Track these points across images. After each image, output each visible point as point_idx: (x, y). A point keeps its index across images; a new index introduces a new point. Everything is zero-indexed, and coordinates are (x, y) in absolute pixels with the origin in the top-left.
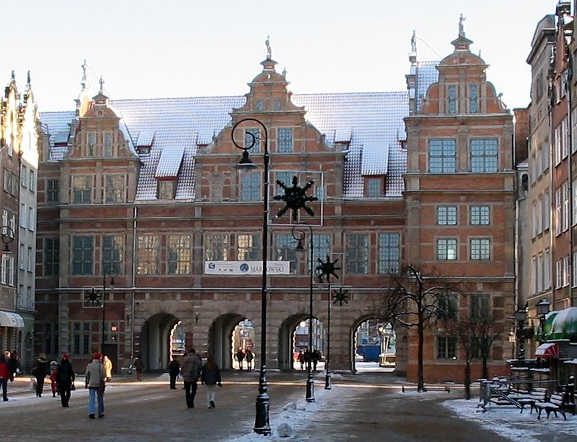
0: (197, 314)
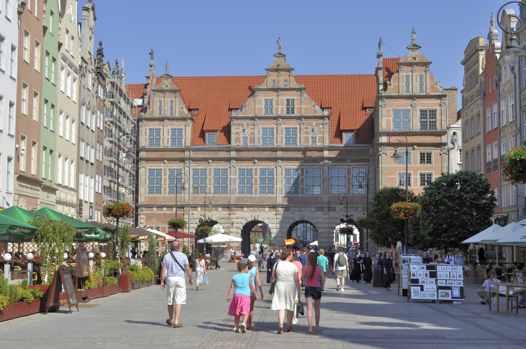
0: (232, 220)
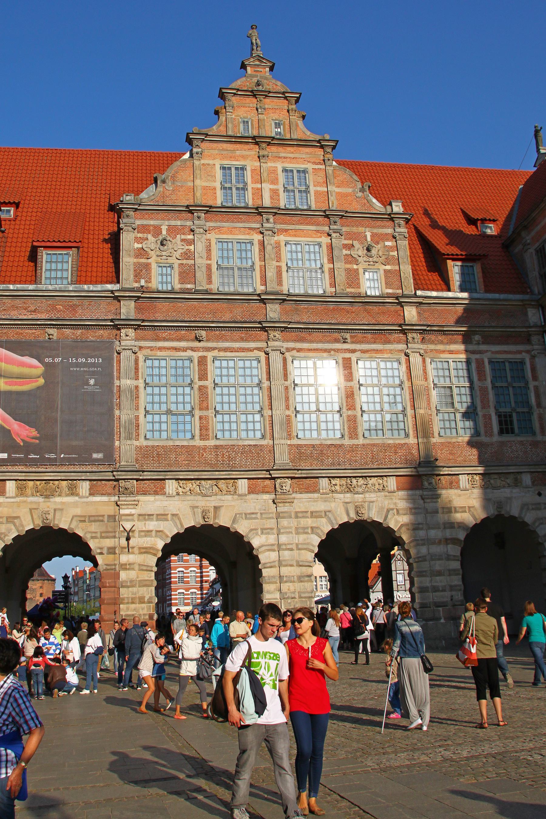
0: (128, 526)
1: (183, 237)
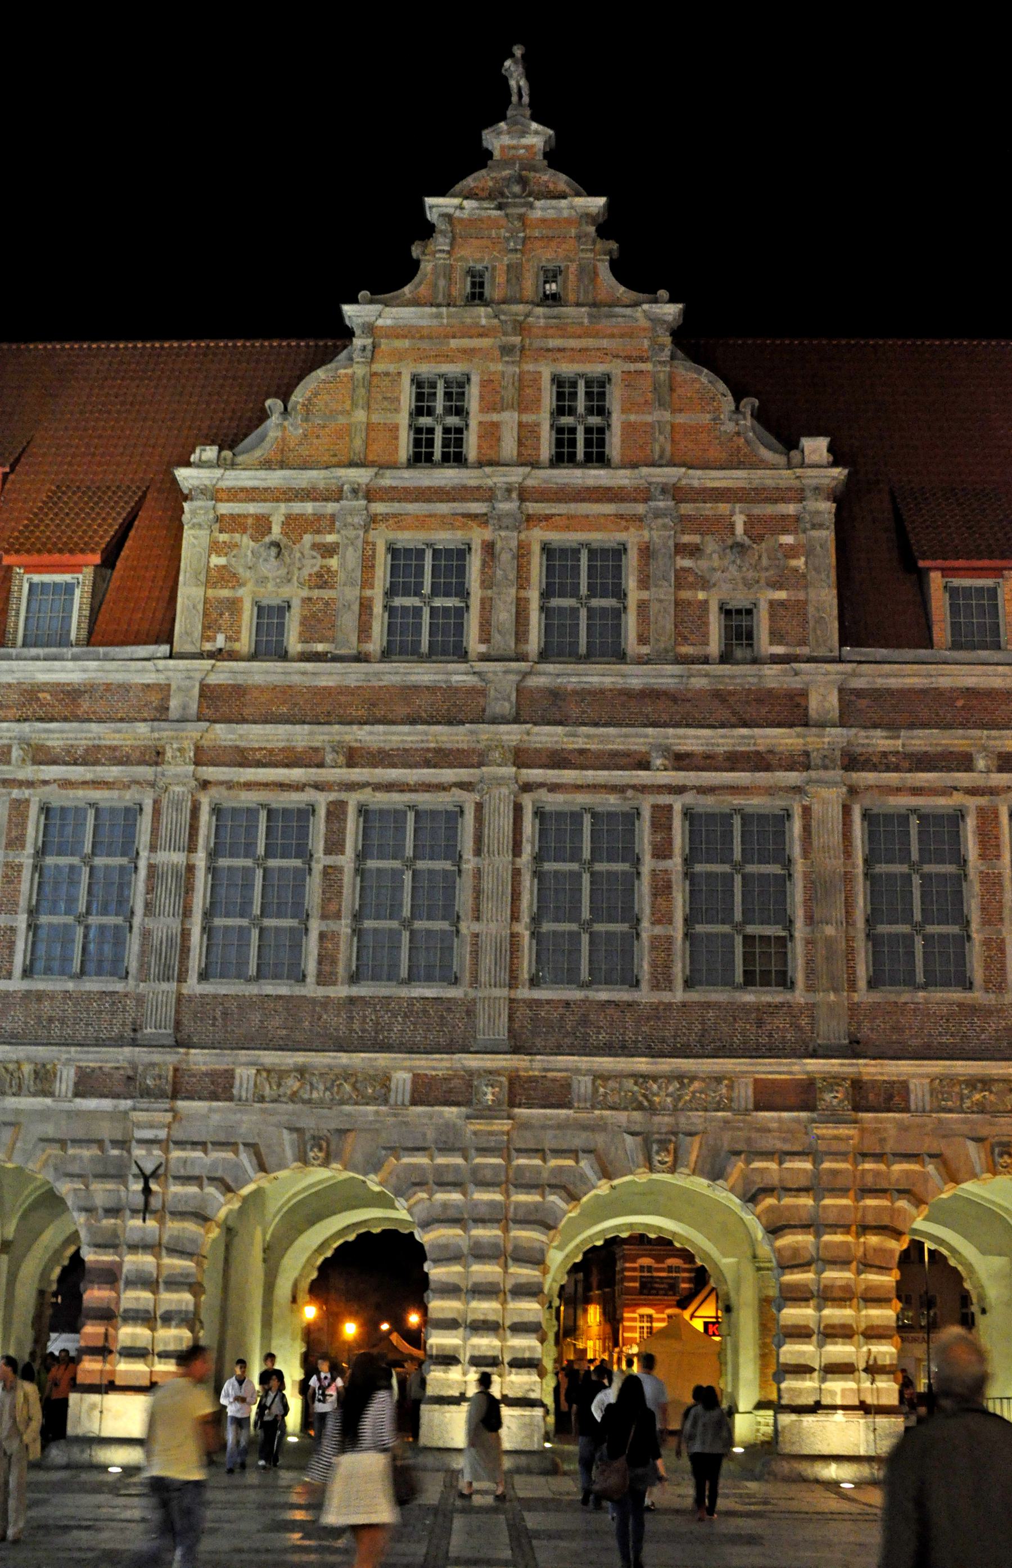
1: (318, 539)
